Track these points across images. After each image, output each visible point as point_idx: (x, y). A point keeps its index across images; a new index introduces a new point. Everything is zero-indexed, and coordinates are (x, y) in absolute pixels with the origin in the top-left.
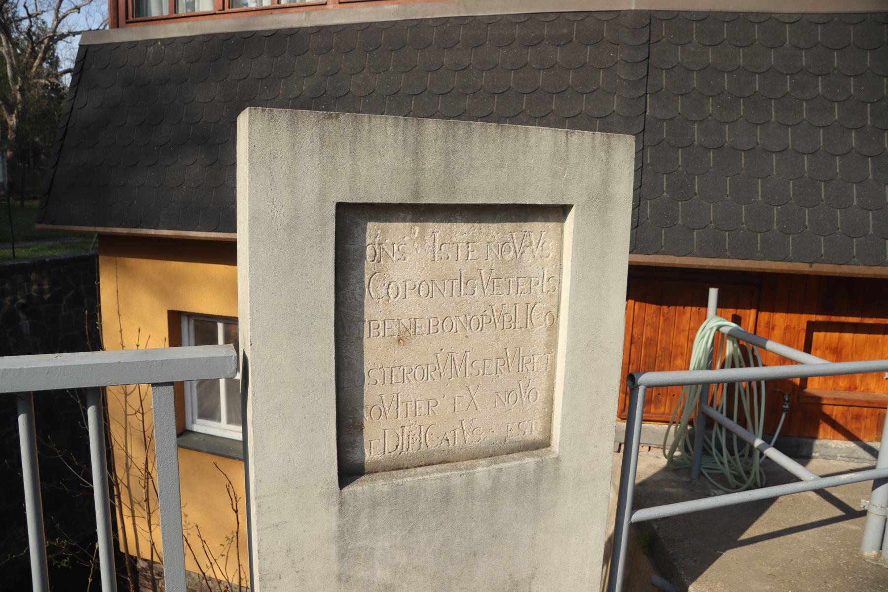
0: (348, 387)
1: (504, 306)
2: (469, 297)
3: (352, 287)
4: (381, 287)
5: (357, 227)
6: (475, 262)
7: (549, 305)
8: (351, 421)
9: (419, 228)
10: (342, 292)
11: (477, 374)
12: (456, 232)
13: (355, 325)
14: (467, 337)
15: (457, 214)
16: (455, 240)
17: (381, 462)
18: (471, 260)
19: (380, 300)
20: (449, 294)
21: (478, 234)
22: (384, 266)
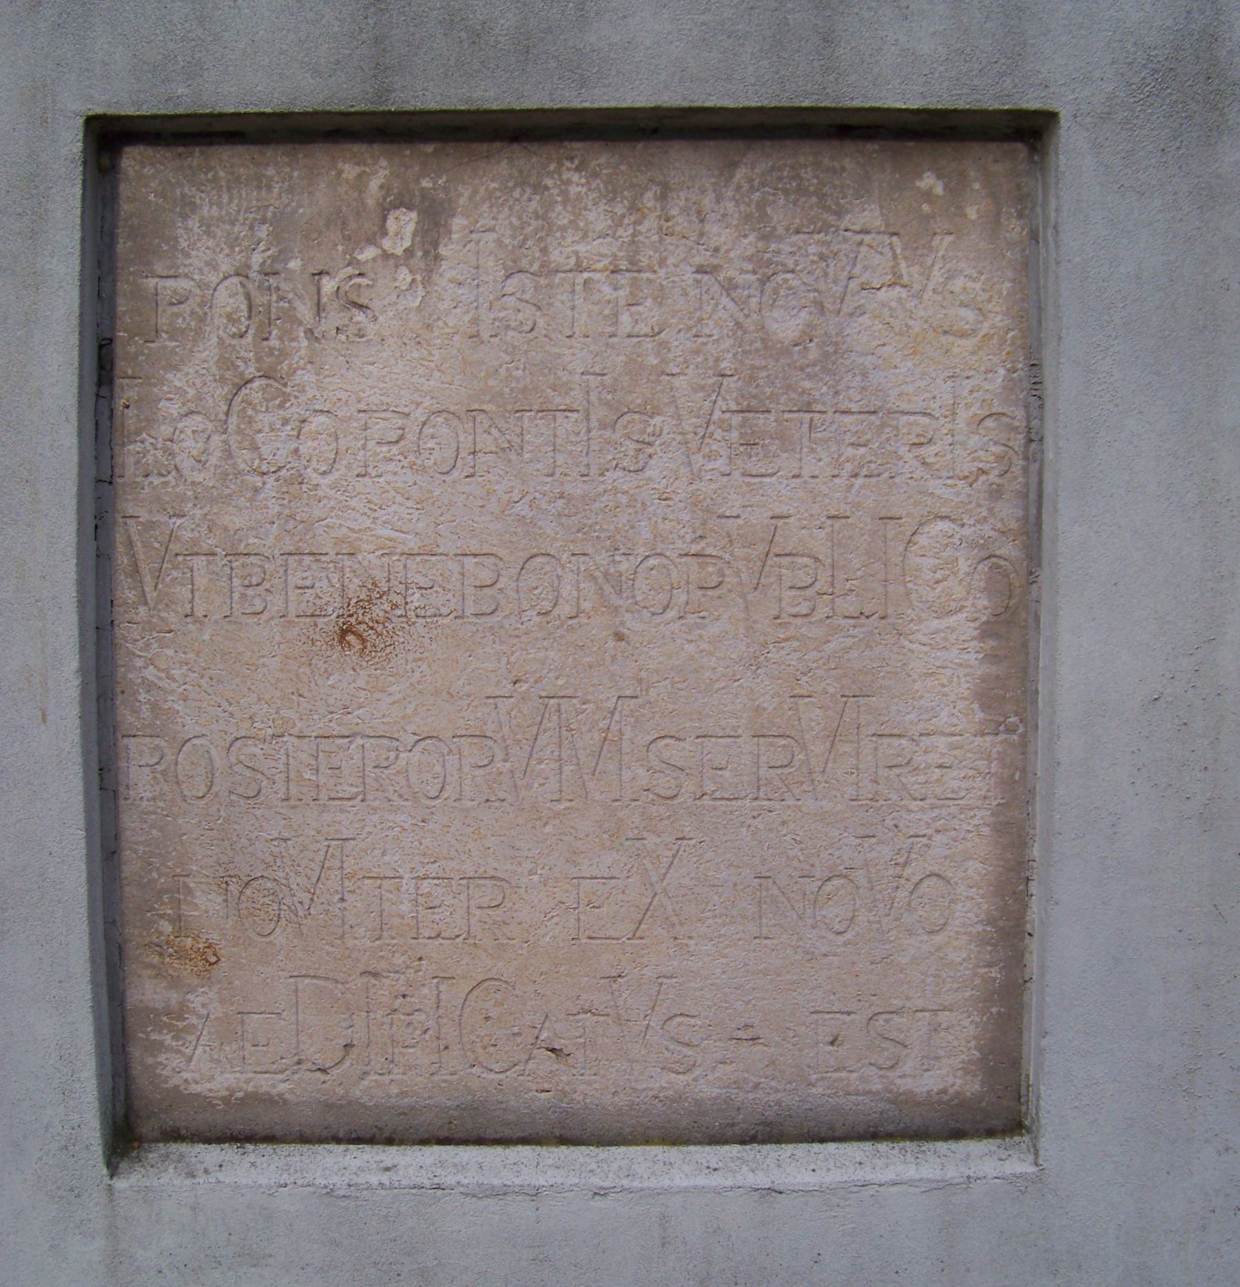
0: (154, 799)
1: (780, 523)
2: (627, 482)
3: (165, 430)
4: (272, 430)
5: (185, 217)
6: (648, 345)
7: (987, 530)
8: (166, 927)
9: (414, 215)
10: (131, 447)
11: (670, 793)
12: (563, 229)
13: (175, 568)
14: (619, 637)
15: (568, 164)
16: (561, 260)
17: (285, 1102)
18: (629, 336)
19: (270, 480)
20: (539, 466)
21: (655, 238)
22: (284, 354)
